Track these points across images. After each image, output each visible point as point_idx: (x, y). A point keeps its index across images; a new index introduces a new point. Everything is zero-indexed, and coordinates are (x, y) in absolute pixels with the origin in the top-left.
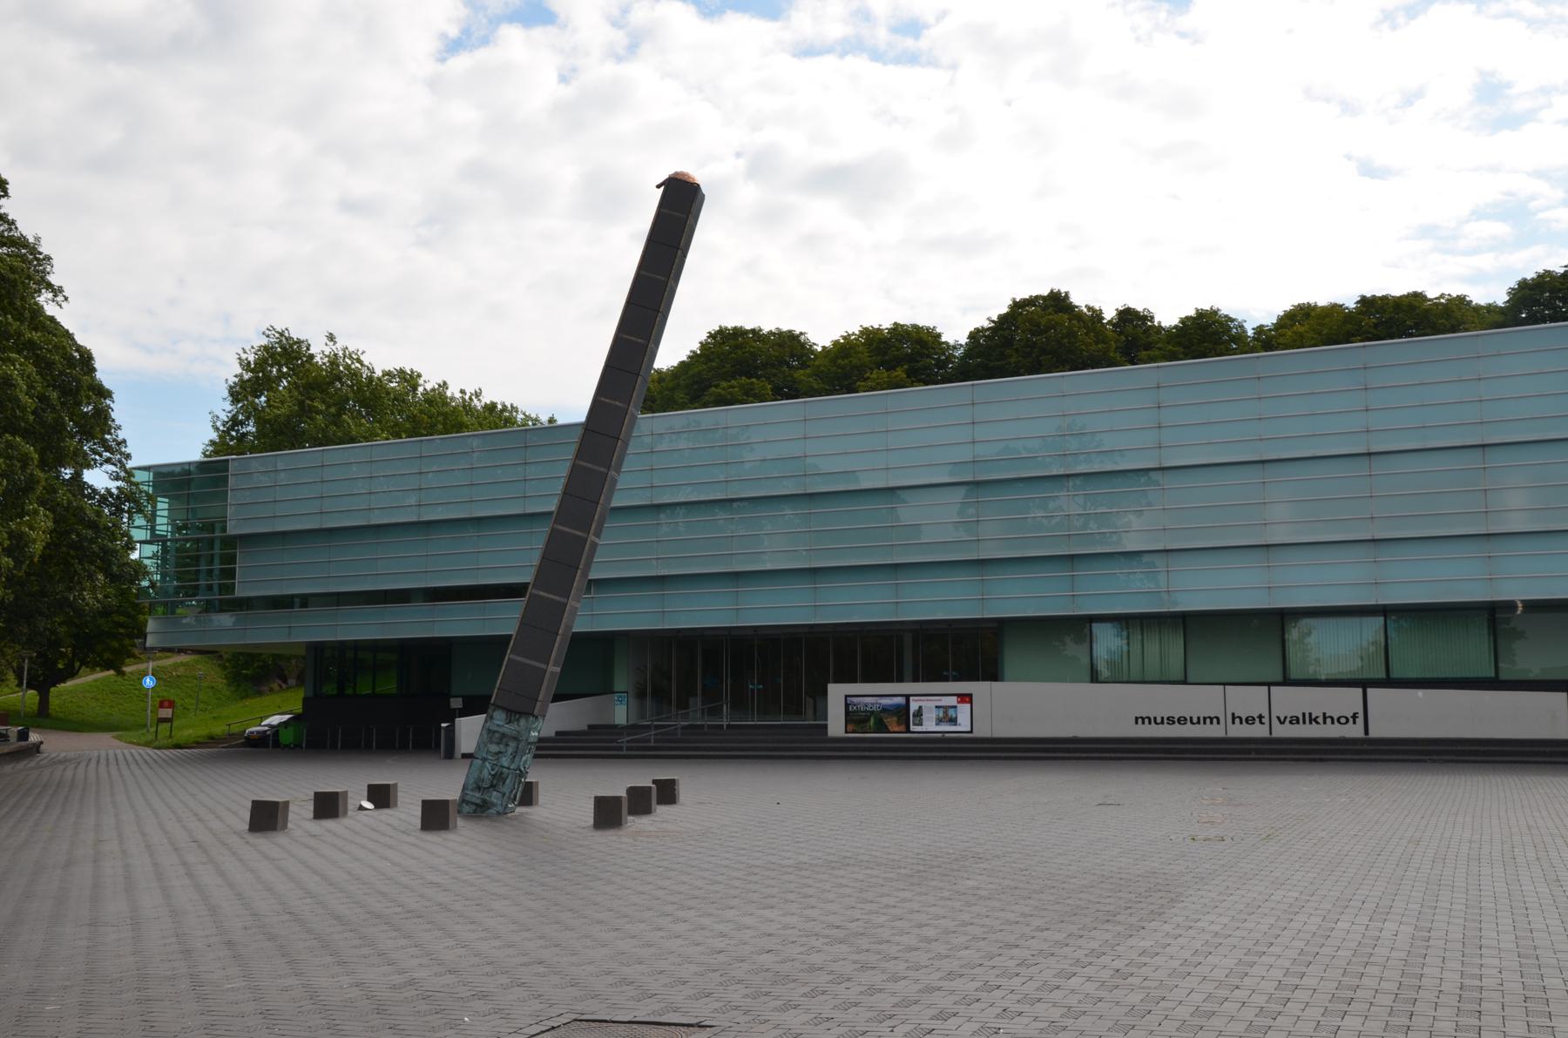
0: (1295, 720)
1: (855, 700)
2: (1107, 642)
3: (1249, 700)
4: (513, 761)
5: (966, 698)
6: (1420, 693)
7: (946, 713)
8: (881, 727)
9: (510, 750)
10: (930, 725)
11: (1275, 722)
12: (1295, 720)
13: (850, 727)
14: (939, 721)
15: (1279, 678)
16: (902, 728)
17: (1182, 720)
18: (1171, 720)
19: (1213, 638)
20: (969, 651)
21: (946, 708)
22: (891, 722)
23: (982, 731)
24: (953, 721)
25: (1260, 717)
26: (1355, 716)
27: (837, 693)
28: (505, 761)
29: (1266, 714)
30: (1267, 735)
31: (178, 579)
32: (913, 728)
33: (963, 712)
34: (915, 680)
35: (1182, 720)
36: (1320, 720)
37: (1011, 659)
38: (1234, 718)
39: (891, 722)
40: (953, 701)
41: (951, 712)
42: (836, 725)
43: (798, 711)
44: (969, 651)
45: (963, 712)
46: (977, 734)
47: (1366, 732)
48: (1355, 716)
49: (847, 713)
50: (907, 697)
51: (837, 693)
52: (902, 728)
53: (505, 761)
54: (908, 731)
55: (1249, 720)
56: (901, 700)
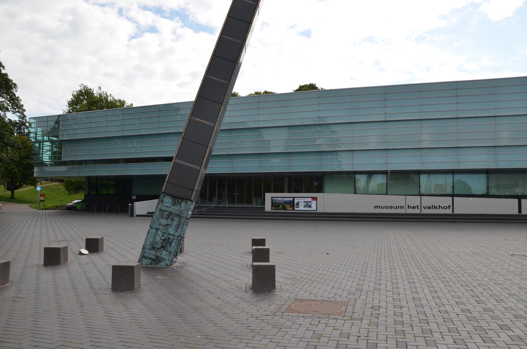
0: (429, 208)
1: (275, 199)
2: (361, 180)
3: (414, 201)
4: (177, 230)
5: (315, 199)
6: (471, 199)
7: (307, 204)
8: (284, 208)
9: (175, 223)
10: (302, 208)
11: (422, 208)
12: (429, 208)
13: (273, 208)
14: (305, 206)
15: (418, 194)
16: (292, 209)
17: (391, 207)
18: (387, 207)
19: (403, 179)
20: (313, 182)
21: (307, 202)
22: (288, 206)
23: (320, 210)
24: (310, 206)
25: (418, 206)
26: (449, 207)
27: (269, 196)
28: (171, 231)
29: (419, 206)
30: (420, 212)
31: (21, 142)
32: (295, 209)
33: (314, 203)
34: (289, 192)
35: (391, 207)
36: (438, 208)
37: (327, 186)
38: (408, 207)
39: (288, 206)
40: (310, 199)
41: (309, 204)
42: (268, 207)
43: (250, 202)
44: (313, 182)
45: (314, 203)
46: (318, 211)
47: (453, 212)
48: (449, 207)
49: (272, 203)
50: (294, 198)
51: (269, 196)
52: (292, 209)
53: (171, 231)
54: (294, 210)
55: (414, 208)
56: (292, 199)
